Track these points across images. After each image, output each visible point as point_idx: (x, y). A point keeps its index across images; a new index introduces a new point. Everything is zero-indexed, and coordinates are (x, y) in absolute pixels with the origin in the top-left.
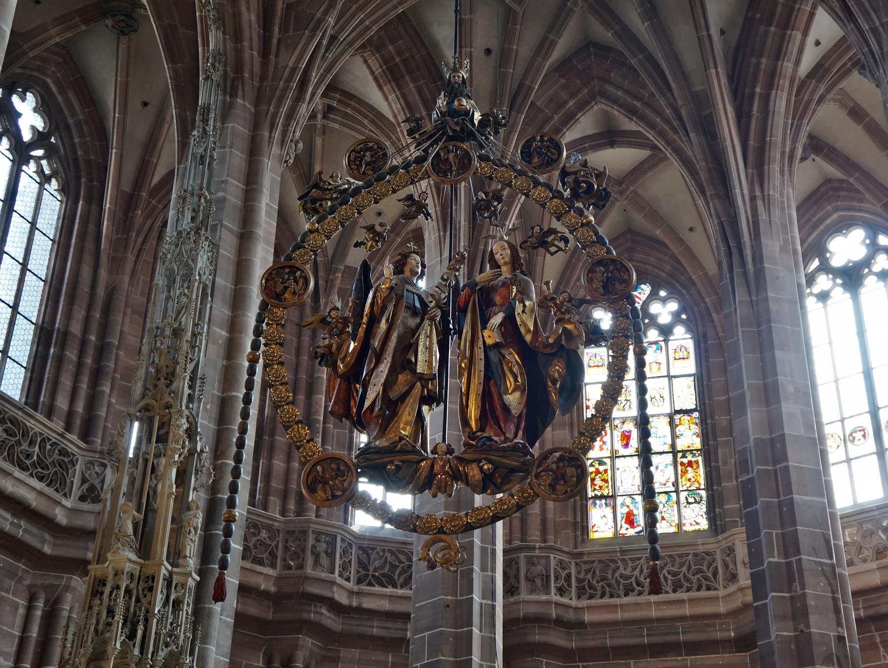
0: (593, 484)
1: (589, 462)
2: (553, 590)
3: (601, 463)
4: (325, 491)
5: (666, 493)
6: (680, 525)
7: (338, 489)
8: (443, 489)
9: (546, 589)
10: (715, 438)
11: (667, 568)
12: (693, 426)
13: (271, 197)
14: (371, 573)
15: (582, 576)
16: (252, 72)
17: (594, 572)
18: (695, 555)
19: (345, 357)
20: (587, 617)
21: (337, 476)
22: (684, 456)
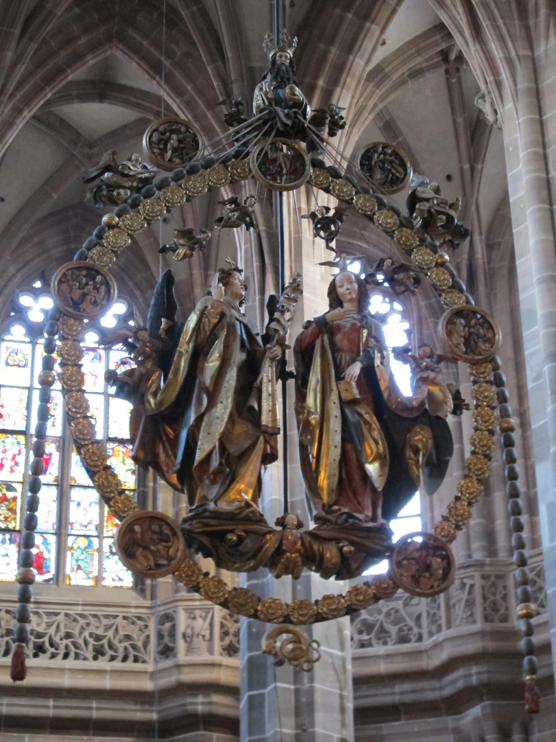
3: (10, 488)
18: (125, 618)
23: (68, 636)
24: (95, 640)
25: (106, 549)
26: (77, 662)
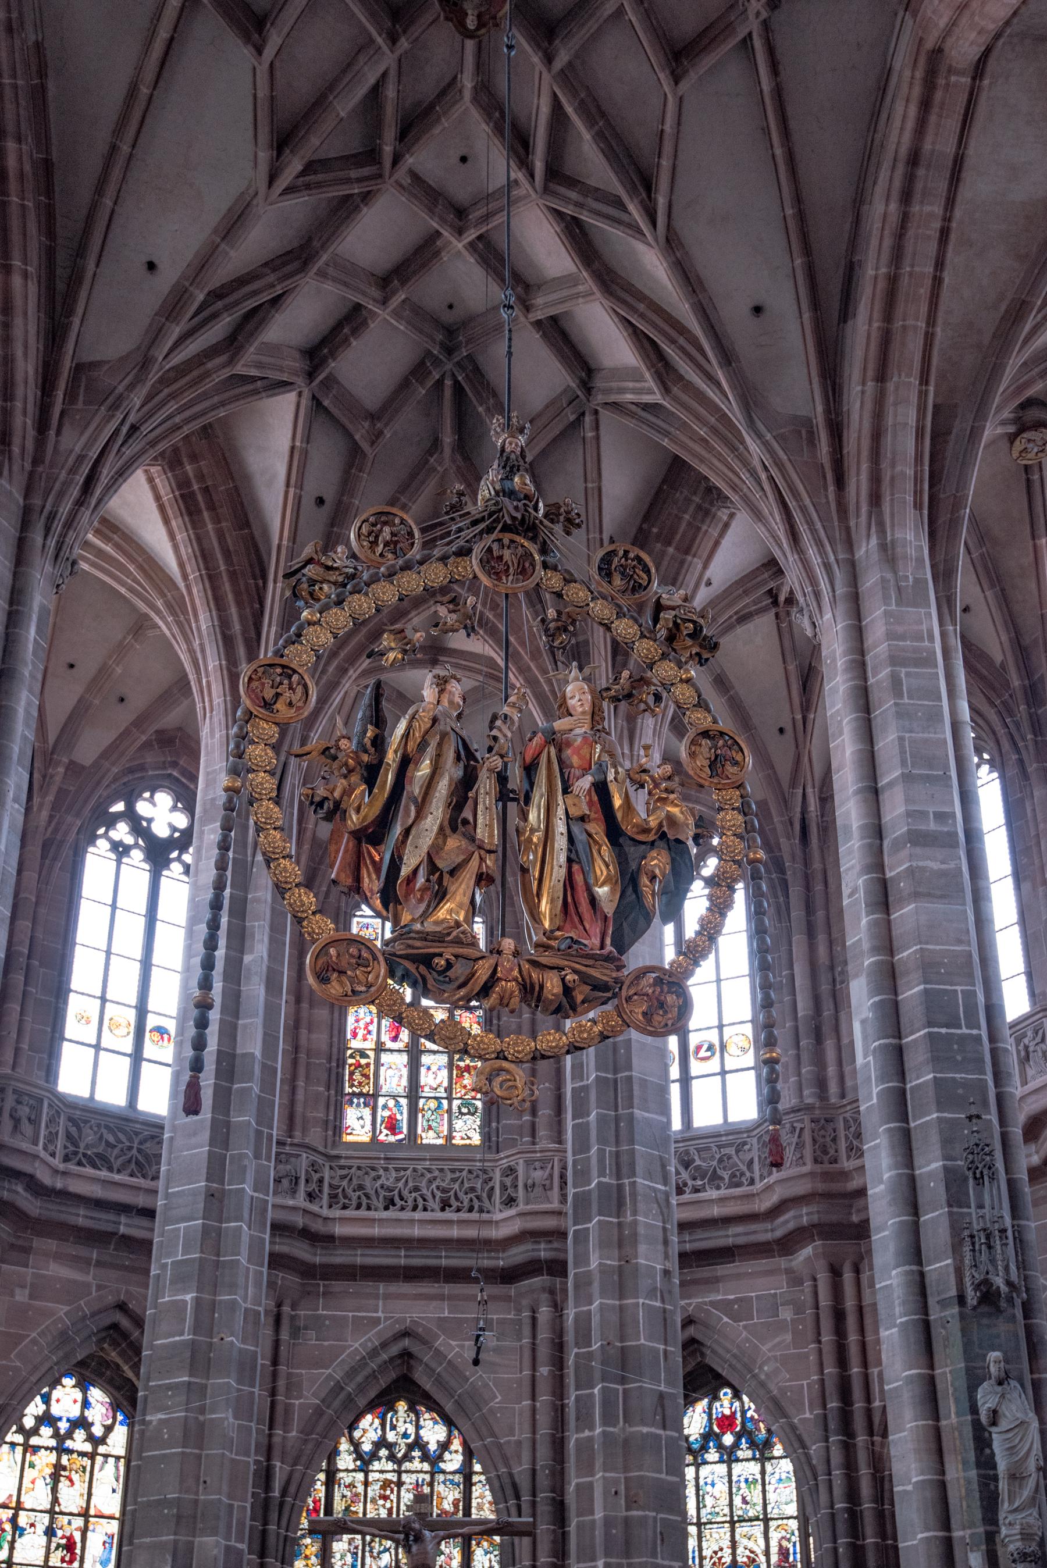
1: (349, 1052)
5: (436, 1098)
6: (450, 1137)
9: (293, 1192)
15: (335, 1182)
18: (470, 1172)
20: (339, 1230)
22: (461, 1059)
23: (416, 1189)
25: (455, 1108)
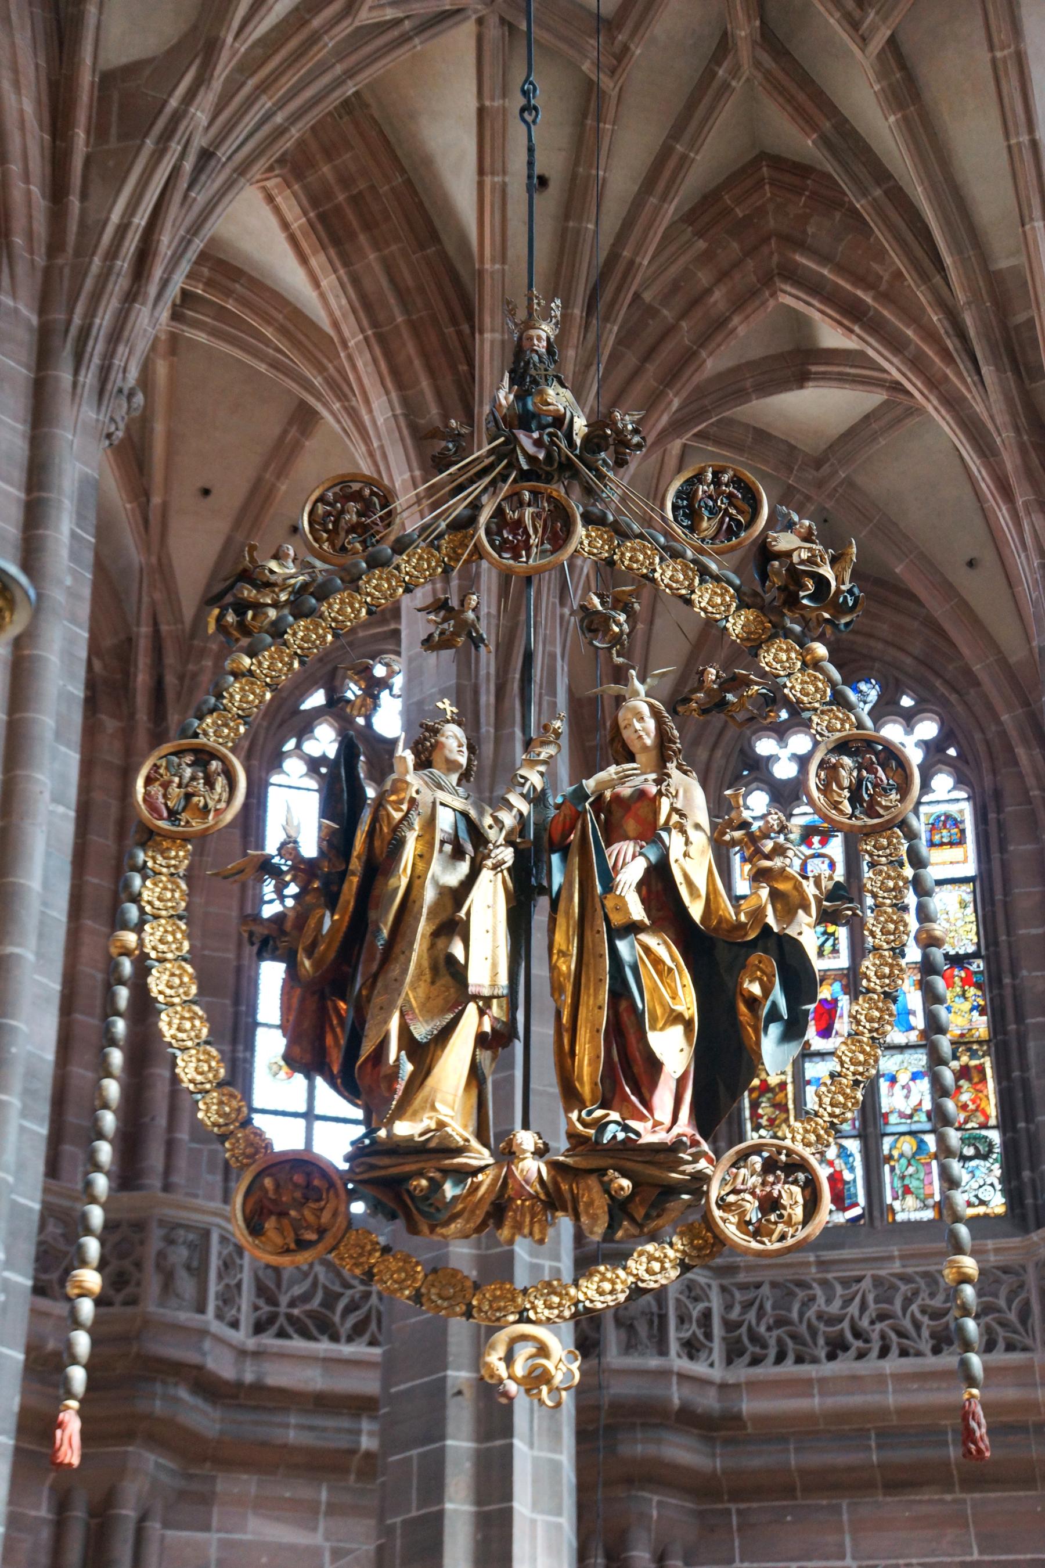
0: (755, 1116)
2: (674, 1346)
4: (280, 1230)
5: (911, 1133)
7: (308, 1227)
8: (526, 1231)
10: (1020, 1018)
11: (919, 1302)
12: (972, 991)
13: (80, 518)
14: (283, 1309)
15: (734, 1315)
16: (30, 235)
17: (761, 1307)
19: (314, 945)
20: (748, 1406)
21: (307, 1199)
24: (931, 1318)
26: (904, 1360)
